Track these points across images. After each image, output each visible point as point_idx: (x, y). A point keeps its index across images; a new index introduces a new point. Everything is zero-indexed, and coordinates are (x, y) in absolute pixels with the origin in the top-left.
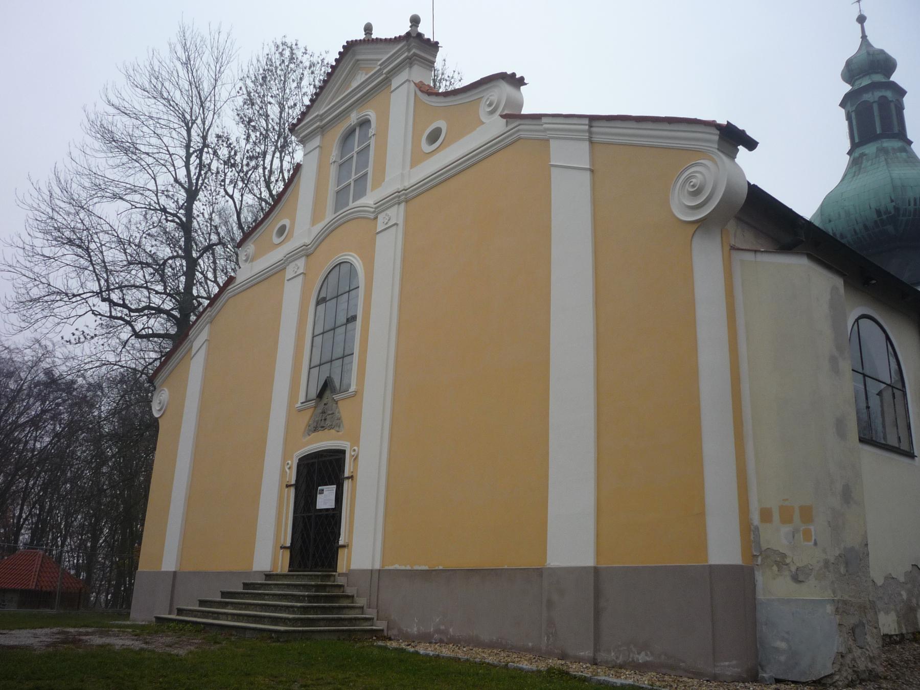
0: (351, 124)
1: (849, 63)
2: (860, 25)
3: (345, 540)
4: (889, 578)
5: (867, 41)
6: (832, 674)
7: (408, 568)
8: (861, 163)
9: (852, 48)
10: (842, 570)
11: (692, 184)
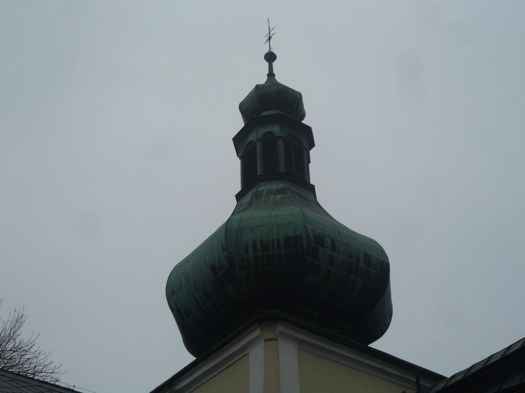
2: (267, 64)
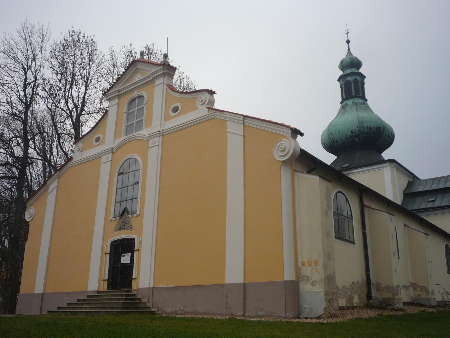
0: (134, 96)
1: (342, 62)
2: (347, 44)
3: (135, 276)
4: (344, 287)
5: (350, 52)
6: (323, 315)
7: (166, 286)
8: (346, 108)
9: (343, 55)
10: (327, 281)
11: (281, 148)
